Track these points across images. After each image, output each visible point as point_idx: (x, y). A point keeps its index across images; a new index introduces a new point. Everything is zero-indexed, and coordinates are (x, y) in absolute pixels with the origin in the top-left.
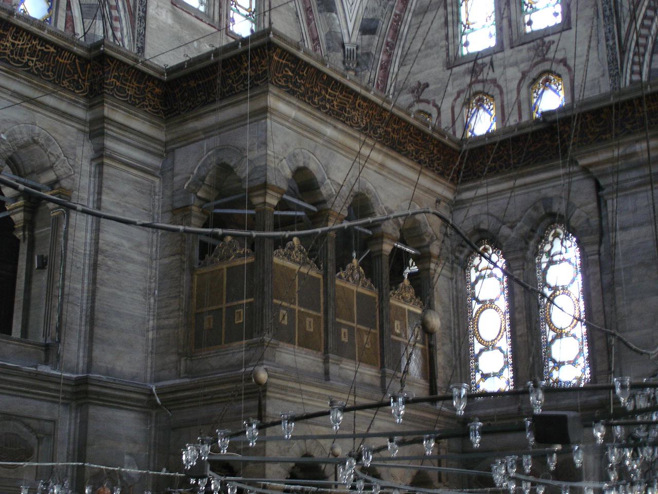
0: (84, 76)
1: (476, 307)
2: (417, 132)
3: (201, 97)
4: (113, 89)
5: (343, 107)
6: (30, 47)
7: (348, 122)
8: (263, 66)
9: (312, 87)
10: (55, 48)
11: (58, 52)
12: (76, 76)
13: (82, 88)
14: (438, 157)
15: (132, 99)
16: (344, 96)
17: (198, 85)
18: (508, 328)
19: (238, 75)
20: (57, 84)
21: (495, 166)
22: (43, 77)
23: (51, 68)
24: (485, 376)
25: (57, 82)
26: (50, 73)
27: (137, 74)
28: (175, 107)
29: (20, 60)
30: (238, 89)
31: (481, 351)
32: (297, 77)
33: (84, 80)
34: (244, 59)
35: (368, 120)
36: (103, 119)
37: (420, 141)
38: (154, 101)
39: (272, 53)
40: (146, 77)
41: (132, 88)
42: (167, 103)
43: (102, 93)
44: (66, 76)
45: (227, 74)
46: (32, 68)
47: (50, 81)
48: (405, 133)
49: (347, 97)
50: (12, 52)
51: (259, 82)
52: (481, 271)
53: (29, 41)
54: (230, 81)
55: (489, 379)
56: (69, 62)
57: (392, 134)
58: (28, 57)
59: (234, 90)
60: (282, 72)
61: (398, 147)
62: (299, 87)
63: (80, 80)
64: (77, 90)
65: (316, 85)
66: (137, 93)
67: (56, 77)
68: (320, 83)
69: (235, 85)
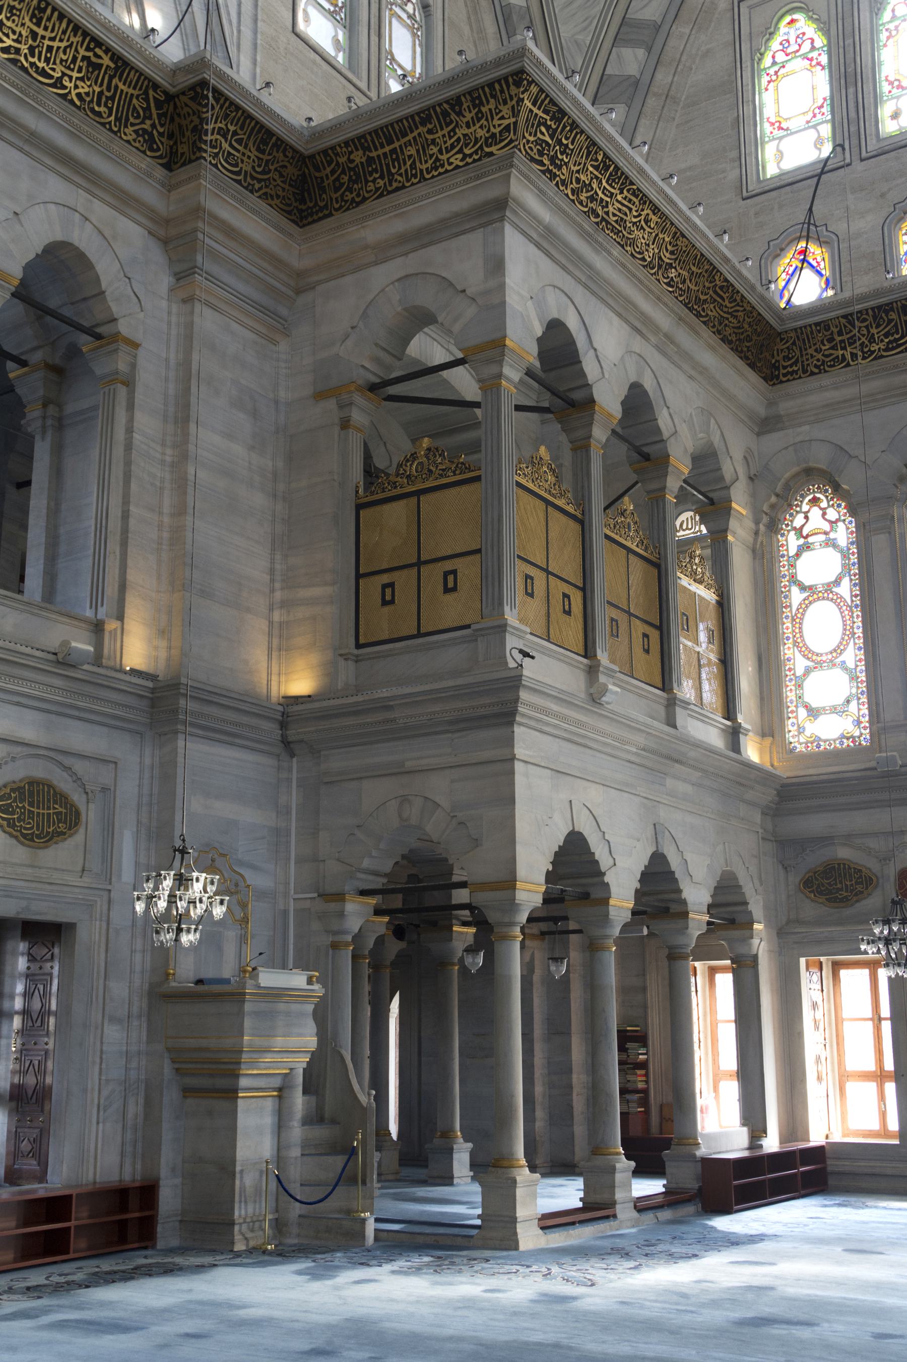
0: (162, 125)
1: (796, 596)
2: (725, 284)
3: (374, 181)
4: (217, 155)
5: (622, 219)
6: (66, 48)
7: (628, 248)
8: (503, 118)
9: (578, 172)
10: (111, 59)
11: (117, 69)
12: (148, 122)
13: (158, 149)
14: (748, 336)
15: (249, 179)
16: (625, 198)
17: (370, 160)
18: (859, 632)
19: (450, 137)
20: (115, 133)
21: (843, 355)
22: (89, 113)
23: (104, 99)
24: (814, 713)
25: (116, 129)
26: (102, 109)
27: (259, 132)
28: (322, 204)
29: (46, 68)
30: (450, 164)
31: (807, 672)
32: (558, 148)
33: (161, 134)
34: (465, 106)
35: (656, 251)
36: (198, 211)
37: (727, 302)
38: (284, 189)
39: (523, 93)
40: (274, 138)
41: (249, 157)
42: (306, 194)
43: (198, 159)
44: (132, 120)
45: (430, 137)
46: (70, 92)
47: (103, 124)
48: (707, 284)
49: (630, 201)
50: (32, 49)
51: (493, 149)
52: (807, 536)
53: (64, 32)
54: (435, 150)
55: (822, 719)
56: (136, 92)
57: (688, 281)
58: (63, 69)
59: (442, 166)
60: (535, 135)
61: (696, 307)
62: (559, 168)
63: (155, 132)
64: (150, 150)
65: (585, 170)
66: (258, 169)
67: (112, 118)
68: (592, 165)
69: (444, 157)
